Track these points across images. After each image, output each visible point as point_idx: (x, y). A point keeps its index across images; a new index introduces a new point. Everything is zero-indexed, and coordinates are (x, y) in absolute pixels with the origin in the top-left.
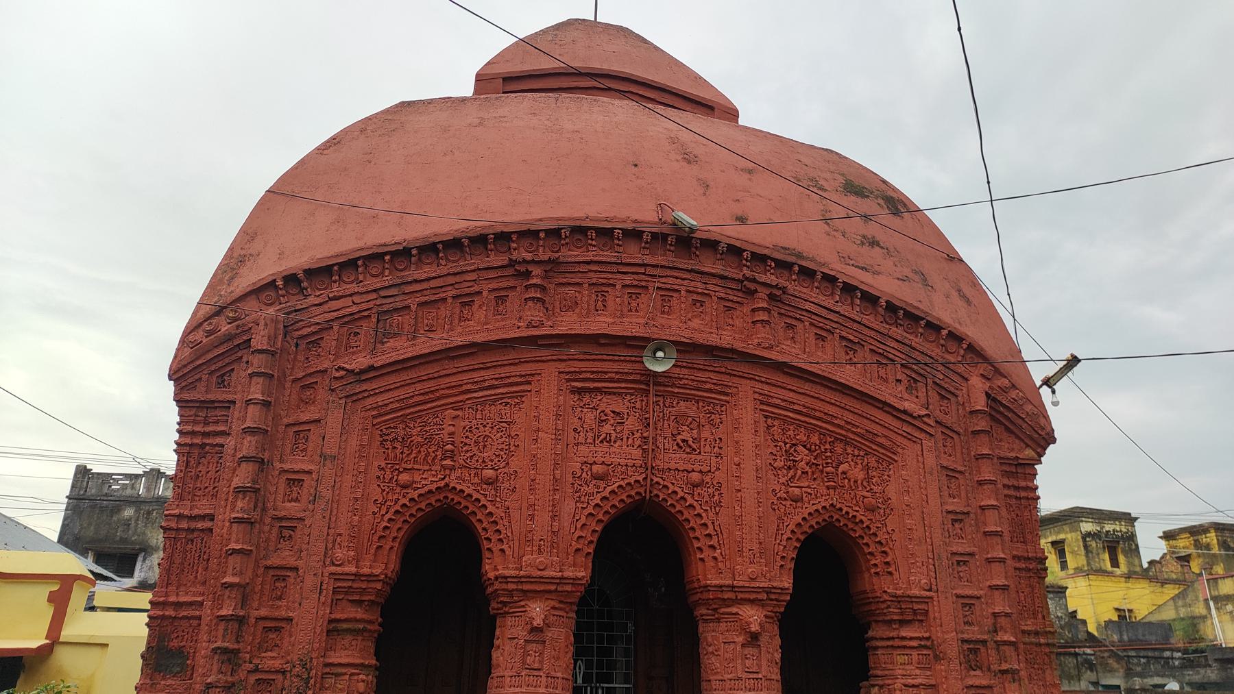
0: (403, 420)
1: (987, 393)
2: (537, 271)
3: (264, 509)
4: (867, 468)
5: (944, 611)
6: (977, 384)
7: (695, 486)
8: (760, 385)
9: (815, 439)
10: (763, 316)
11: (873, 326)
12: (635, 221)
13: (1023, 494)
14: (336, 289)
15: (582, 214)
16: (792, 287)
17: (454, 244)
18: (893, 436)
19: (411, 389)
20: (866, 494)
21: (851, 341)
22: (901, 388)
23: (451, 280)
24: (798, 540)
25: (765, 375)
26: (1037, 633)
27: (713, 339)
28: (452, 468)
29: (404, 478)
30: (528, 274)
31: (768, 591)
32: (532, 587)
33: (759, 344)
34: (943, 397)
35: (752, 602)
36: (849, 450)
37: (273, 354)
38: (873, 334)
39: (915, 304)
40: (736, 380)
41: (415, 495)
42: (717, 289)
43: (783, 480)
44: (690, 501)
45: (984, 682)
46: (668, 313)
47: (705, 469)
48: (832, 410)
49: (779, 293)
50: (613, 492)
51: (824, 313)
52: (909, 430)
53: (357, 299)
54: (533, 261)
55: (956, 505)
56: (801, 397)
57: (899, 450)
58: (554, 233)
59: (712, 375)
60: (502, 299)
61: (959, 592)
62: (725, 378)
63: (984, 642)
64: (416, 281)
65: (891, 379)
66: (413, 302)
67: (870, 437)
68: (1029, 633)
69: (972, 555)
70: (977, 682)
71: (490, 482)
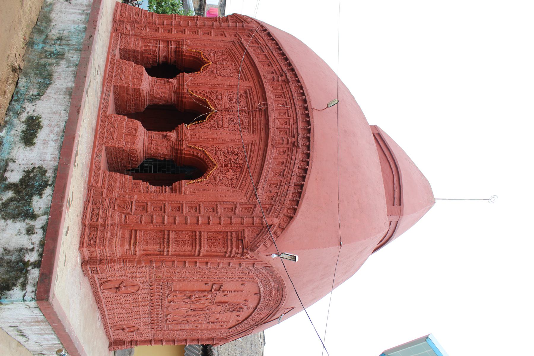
0: (229, 54)
1: (270, 225)
2: (284, 78)
3: (200, 28)
4: (232, 179)
5: (175, 197)
6: (276, 221)
7: (217, 123)
8: (258, 142)
9: (241, 162)
10: (285, 141)
11: (292, 180)
12: (310, 102)
13: (229, 242)
14: (265, 38)
15: (308, 88)
16: (300, 150)
17: (286, 59)
18: (246, 187)
19: (238, 54)
20: (221, 178)
21: (283, 173)
22: (268, 193)
23: (275, 61)
24: (201, 154)
25: (262, 143)
26: (168, 239)
27: (271, 125)
28: (216, 64)
29: (212, 54)
30: (282, 76)
31: (181, 141)
32: (181, 84)
33: (273, 137)
34: (267, 210)
35: (178, 137)
36: (238, 173)
37: (243, 27)
38: (288, 180)
39: (306, 195)
40: (259, 134)
41: (207, 56)
42: (293, 127)
43: (223, 149)
44: (212, 121)
45: (149, 210)
46: (279, 115)
47: (224, 126)
48: (253, 166)
49: (296, 144)
50: (212, 100)
51: (293, 162)
52: (250, 193)
53: (263, 42)
54: (286, 76)
55: (220, 209)
56: (256, 155)
57: (240, 190)
58: (298, 81)
59: (259, 127)
60: (273, 73)
61: (184, 205)
62: (259, 131)
63: (165, 212)
64: (272, 53)
65: (271, 189)
66: (266, 53)
67: (245, 179)
68: (169, 235)
69: (200, 213)
70: (149, 207)
71: (212, 72)
